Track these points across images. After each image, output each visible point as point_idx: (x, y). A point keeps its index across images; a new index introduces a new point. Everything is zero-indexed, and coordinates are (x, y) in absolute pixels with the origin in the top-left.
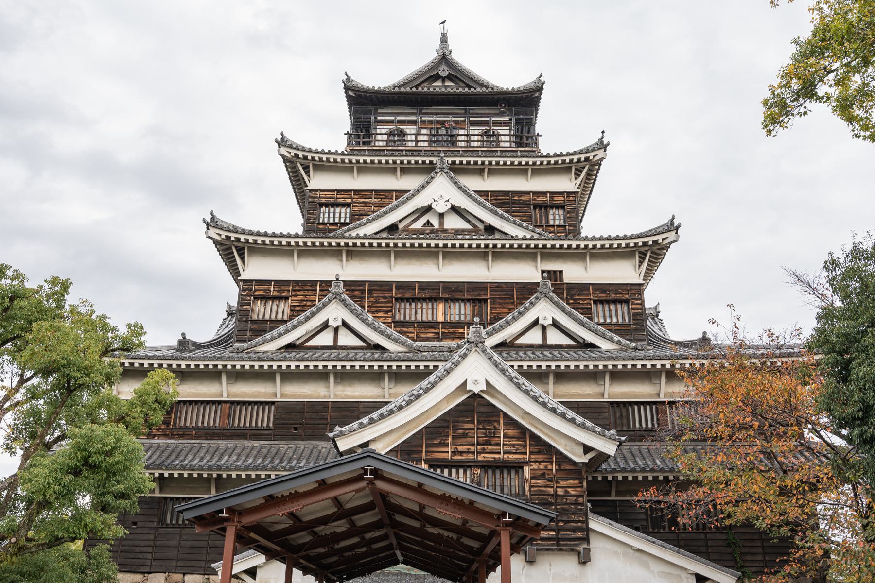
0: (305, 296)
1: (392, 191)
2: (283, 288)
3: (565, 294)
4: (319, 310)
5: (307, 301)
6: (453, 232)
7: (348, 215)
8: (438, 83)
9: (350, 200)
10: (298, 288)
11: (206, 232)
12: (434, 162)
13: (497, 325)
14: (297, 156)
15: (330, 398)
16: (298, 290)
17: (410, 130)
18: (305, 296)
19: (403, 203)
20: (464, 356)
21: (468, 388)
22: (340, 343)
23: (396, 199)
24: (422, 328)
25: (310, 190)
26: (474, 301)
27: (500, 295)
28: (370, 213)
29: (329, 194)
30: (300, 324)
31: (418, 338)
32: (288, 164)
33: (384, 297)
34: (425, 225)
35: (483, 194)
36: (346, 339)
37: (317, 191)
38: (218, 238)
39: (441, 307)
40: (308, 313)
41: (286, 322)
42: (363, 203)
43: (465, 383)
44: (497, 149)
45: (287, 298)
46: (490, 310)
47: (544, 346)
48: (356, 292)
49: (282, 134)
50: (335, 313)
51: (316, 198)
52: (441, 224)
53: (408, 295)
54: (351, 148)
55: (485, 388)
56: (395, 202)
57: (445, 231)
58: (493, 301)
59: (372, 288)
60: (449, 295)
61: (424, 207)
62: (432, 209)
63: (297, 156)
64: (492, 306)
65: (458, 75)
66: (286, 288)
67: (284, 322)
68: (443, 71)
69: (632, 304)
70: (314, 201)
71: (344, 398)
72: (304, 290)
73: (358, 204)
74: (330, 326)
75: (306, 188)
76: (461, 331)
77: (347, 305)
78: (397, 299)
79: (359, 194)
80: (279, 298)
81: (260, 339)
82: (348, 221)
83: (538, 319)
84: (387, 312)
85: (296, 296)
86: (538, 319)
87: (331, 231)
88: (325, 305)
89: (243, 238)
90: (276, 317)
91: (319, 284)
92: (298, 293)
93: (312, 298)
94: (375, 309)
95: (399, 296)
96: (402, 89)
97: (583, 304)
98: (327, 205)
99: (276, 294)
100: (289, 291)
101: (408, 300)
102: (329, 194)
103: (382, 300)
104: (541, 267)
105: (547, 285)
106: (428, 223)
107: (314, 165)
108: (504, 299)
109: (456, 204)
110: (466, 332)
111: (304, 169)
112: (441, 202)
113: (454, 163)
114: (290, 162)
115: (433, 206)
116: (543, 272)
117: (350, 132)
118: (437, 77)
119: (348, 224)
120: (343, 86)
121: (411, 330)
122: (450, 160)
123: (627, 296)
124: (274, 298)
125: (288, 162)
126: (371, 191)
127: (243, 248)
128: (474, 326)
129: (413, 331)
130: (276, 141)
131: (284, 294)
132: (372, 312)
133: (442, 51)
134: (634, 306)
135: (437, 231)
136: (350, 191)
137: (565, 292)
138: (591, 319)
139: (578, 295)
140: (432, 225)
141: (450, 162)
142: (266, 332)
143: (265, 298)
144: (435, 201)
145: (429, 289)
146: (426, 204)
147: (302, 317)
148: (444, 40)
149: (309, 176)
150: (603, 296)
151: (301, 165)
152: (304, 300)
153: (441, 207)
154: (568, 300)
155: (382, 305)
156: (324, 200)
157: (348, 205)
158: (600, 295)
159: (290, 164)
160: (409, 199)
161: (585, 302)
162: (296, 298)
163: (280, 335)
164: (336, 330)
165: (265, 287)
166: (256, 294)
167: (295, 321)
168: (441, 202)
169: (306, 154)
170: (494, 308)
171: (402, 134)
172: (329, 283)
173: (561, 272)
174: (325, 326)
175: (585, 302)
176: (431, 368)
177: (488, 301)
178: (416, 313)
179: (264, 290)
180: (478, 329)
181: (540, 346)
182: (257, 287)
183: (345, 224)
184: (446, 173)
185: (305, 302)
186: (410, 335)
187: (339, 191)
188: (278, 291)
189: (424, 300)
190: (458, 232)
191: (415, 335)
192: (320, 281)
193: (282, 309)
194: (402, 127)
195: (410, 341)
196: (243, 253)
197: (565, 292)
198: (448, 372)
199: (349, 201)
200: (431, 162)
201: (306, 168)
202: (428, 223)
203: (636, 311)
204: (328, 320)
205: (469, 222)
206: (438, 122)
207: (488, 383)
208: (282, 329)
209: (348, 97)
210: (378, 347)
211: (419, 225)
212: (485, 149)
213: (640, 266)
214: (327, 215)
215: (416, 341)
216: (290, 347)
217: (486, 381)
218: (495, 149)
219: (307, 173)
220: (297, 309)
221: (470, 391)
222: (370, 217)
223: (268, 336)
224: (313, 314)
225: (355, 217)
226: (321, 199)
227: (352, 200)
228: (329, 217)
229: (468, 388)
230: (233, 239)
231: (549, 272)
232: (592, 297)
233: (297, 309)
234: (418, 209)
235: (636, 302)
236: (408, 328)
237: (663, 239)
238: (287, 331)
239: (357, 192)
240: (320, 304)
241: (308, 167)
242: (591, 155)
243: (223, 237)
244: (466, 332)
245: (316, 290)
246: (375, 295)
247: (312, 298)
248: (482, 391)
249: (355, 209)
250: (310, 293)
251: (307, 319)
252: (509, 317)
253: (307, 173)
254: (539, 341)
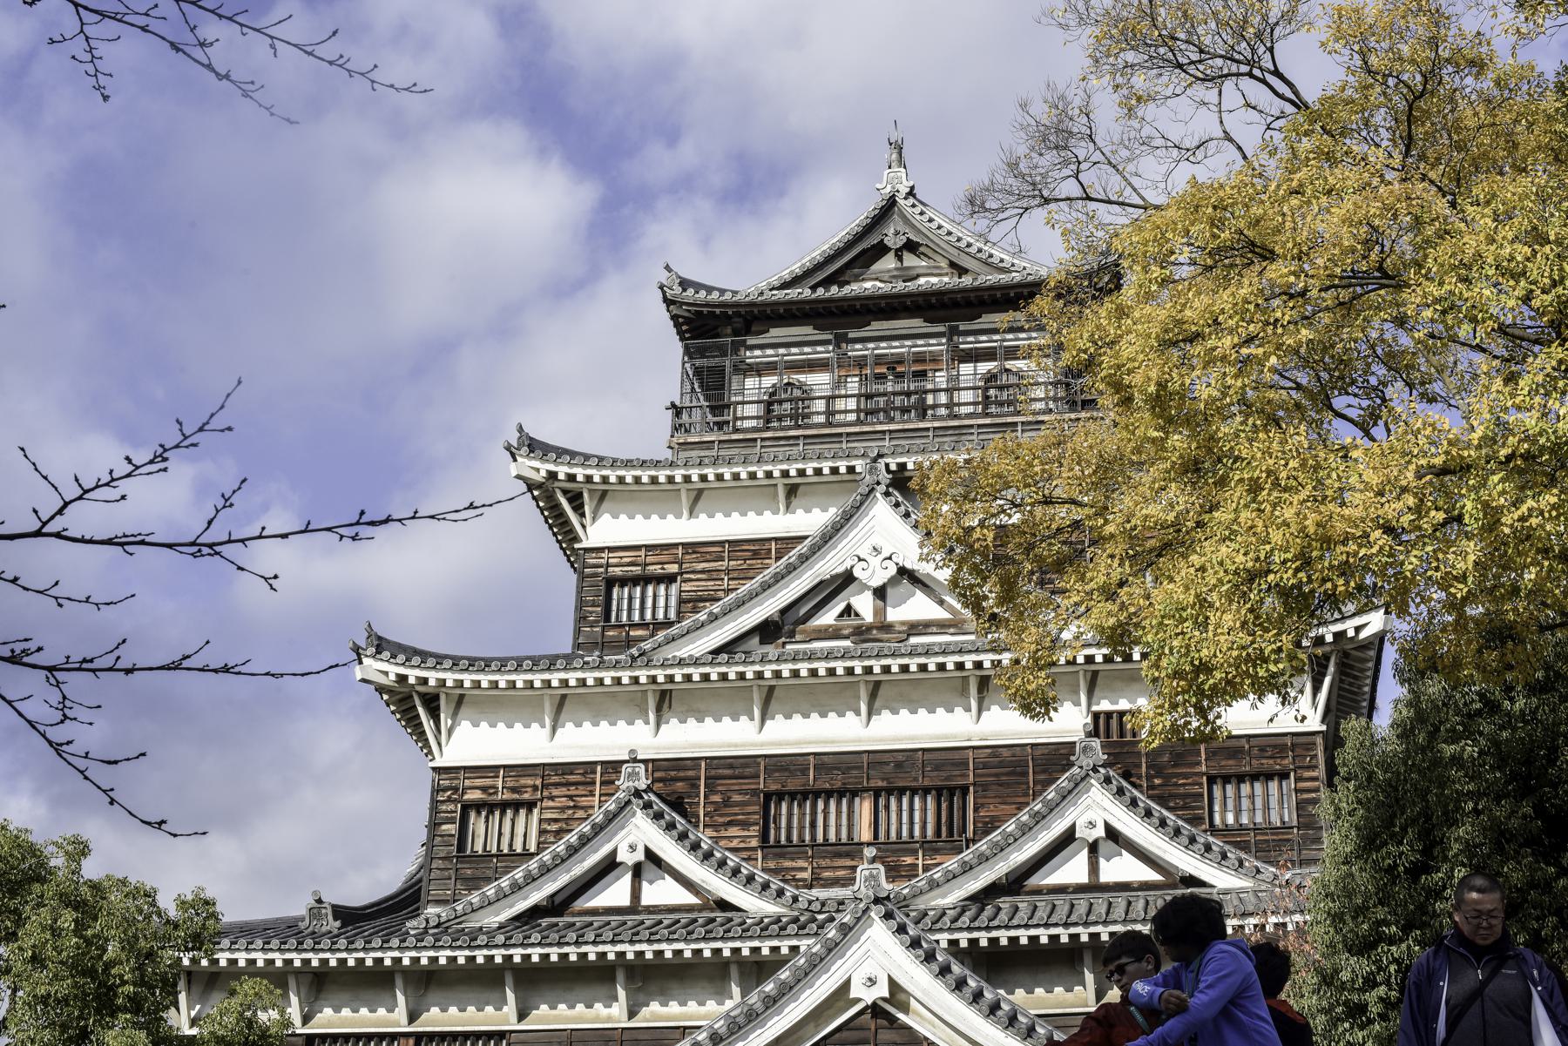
0: (571, 797)
1: (769, 540)
2: (523, 781)
3: (1144, 765)
4: (598, 829)
5: (575, 807)
6: (905, 628)
7: (673, 602)
8: (888, 263)
9: (676, 566)
10: (555, 779)
12: (858, 469)
13: (982, 846)
14: (552, 476)
15: (620, 1022)
16: (556, 785)
17: (819, 381)
18: (571, 797)
19: (791, 569)
20: (845, 930)
21: (854, 993)
23: (778, 559)
24: (824, 858)
25: (586, 550)
26: (939, 791)
27: (996, 775)
28: (721, 594)
29: (628, 556)
30: (561, 861)
31: (816, 881)
32: (536, 493)
33: (740, 792)
34: (841, 615)
37: (601, 550)
38: (382, 680)
39: (864, 808)
40: (572, 838)
41: (533, 855)
42: (702, 572)
43: (846, 985)
44: (1015, 419)
45: (530, 806)
46: (976, 810)
47: (1094, 887)
48: (680, 784)
49: (520, 429)
51: (601, 567)
52: (880, 613)
53: (793, 784)
54: (681, 441)
55: (886, 994)
56: (775, 567)
57: (887, 627)
58: (982, 787)
59: (713, 772)
60: (883, 780)
61: (837, 576)
62: (856, 579)
63: (552, 476)
64: (980, 801)
66: (529, 782)
67: (527, 855)
68: (897, 233)
69: (1297, 780)
70: (595, 575)
71: (648, 1021)
72: (568, 784)
73: (692, 576)
74: (621, 863)
75: (577, 546)
76: (909, 860)
77: (658, 816)
78: (768, 796)
79: (694, 552)
80: (516, 806)
81: (475, 898)
82: (672, 615)
83: (1072, 829)
84: (745, 825)
85: (552, 798)
86: (1072, 829)
87: (630, 642)
88: (611, 818)
89: (433, 677)
90: (511, 845)
91: (599, 768)
92: (555, 792)
93: (584, 801)
94: (721, 820)
95: (773, 787)
96: (793, 294)
97: (1184, 785)
98: (623, 581)
99: (507, 796)
100: (535, 788)
101: (792, 796)
102: (628, 556)
103: (736, 798)
104: (1089, 705)
105: (1091, 749)
106: (848, 610)
107: (590, 491)
108: (1008, 785)
109: (908, 566)
110: (920, 862)
111: (570, 501)
112: (875, 561)
113: (902, 466)
114: (540, 486)
115: (857, 573)
117: (678, 403)
118: (881, 250)
119: (668, 624)
121: (801, 863)
122: (893, 463)
123: (1286, 762)
124: (504, 806)
125: (536, 489)
126: (721, 543)
127: (436, 697)
128: (866, 866)
129: (806, 865)
130: (508, 448)
131: (526, 796)
132: (715, 827)
134: (1302, 785)
135: (870, 628)
136: (675, 545)
137: (1144, 760)
138: (1194, 821)
139: (1173, 766)
140: (857, 615)
141: (893, 467)
142: (488, 880)
143: (488, 807)
144: (860, 560)
145: (838, 769)
146: (840, 569)
147: (560, 847)
149: (583, 515)
150: (1230, 766)
151: (565, 492)
152: (569, 808)
153: (877, 574)
154: (1149, 778)
155: (736, 810)
156: (617, 571)
157: (670, 579)
158: (1223, 763)
159: (544, 492)
160: (804, 559)
161: (1190, 781)
162: (551, 804)
163: (516, 887)
165: (488, 782)
166: (466, 797)
167: (546, 856)
170: (983, 805)
171: (807, 396)
172: (613, 767)
174: (610, 866)
175: (1190, 781)
176: (785, 951)
177: (971, 789)
178: (813, 825)
179: (484, 789)
180: (875, 872)
181: (1080, 889)
182: (467, 783)
183: (658, 626)
184: (887, 494)
185: (570, 812)
186: (800, 875)
187: (649, 548)
188: (514, 790)
189: (828, 794)
190: (916, 628)
191: (806, 875)
192: (603, 763)
193: (524, 829)
194: (802, 377)
195: (790, 891)
196: (438, 708)
197: (1144, 760)
198: (816, 964)
199: (674, 568)
200: (851, 470)
201: (576, 500)
202: (848, 610)
203: (1306, 796)
204: (614, 852)
205: (941, 603)
206: (879, 361)
207: (893, 984)
208: (518, 874)
209: (674, 318)
210: (724, 905)
211: (828, 617)
212: (988, 421)
213: (1316, 689)
215: (810, 887)
216: (535, 912)
217: (890, 978)
218: (1009, 420)
219: (579, 508)
220: (554, 827)
221: (858, 1000)
222: (716, 608)
223: (490, 890)
224: (585, 841)
225: (688, 604)
226: (610, 569)
227: (681, 567)
228: (630, 609)
229: (853, 995)
230: (412, 680)
232: (1204, 769)
233: (554, 827)
234: (821, 582)
235: (1307, 774)
236: (793, 859)
237: (1358, 629)
238: (531, 879)
239: (691, 547)
240: (598, 816)
241: (580, 495)
243: (392, 677)
244: (920, 862)
245: (594, 783)
246: (720, 788)
247: (584, 801)
248: (884, 999)
249: (686, 587)
250: (581, 790)
251: (573, 851)
252: (1010, 827)
253: (579, 508)
254: (1083, 878)
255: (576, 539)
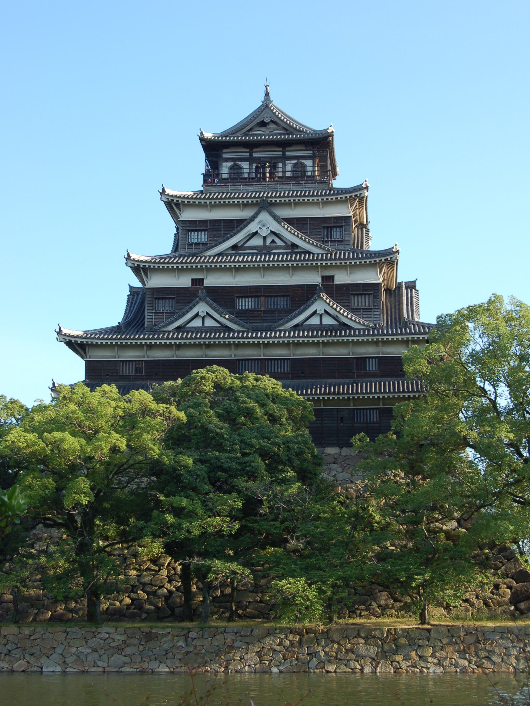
11: (126, 263)
22: (206, 325)
23: (237, 227)
35: (290, 221)
36: (209, 323)
50: (202, 308)
65: (276, 122)
89: (147, 265)
116: (323, 277)
120: (198, 138)
133: (265, 102)
146: (255, 231)
148: (267, 94)
164: (203, 318)
168: (264, 229)
169: (178, 199)
171: (240, 168)
173: (333, 277)
214: (194, 237)
231: (326, 277)
234: (249, 234)
242: (358, 193)
243: (136, 265)
255: (179, 218)
